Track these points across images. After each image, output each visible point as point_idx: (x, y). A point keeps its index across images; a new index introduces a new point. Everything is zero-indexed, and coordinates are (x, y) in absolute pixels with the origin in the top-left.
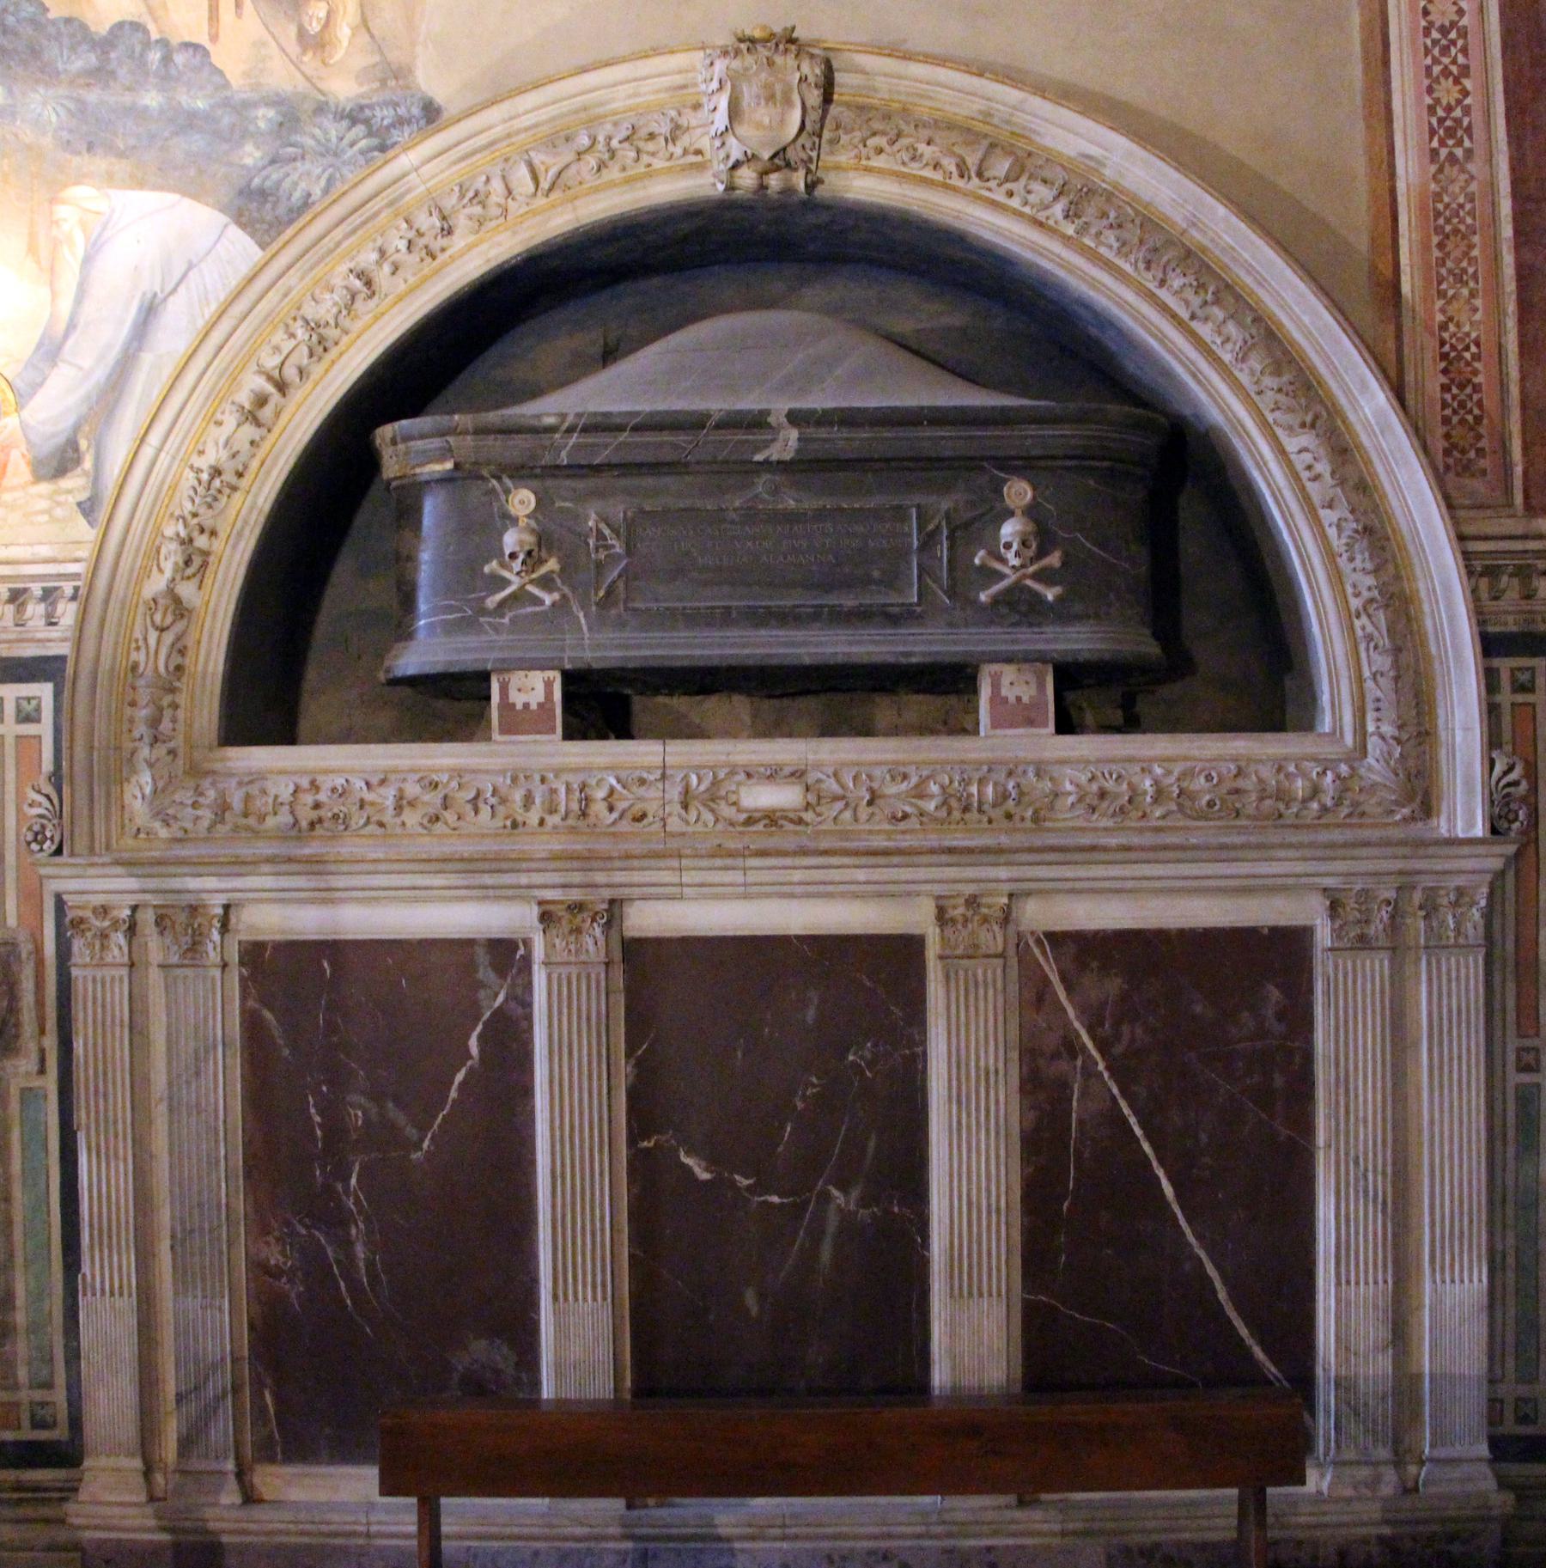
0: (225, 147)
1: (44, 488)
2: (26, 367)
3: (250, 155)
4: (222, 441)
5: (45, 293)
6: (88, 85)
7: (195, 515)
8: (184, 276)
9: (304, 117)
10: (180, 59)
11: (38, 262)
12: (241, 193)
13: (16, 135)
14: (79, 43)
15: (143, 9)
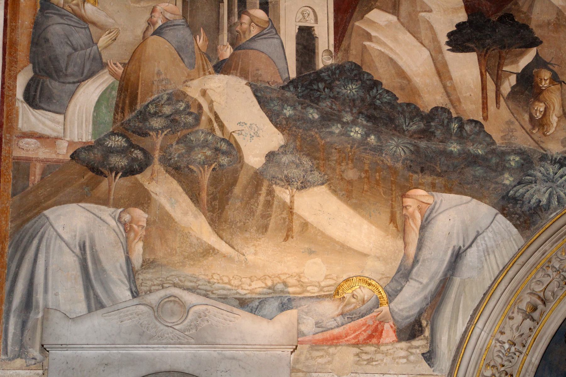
0: (494, 174)
1: (404, 344)
2: (392, 281)
3: (507, 179)
4: (515, 327)
5: (400, 243)
6: (420, 138)
7: (503, 366)
8: (475, 238)
9: (535, 161)
10: (468, 128)
11: (397, 227)
12: (503, 198)
13: (382, 161)
14: (415, 117)
15: (447, 101)
